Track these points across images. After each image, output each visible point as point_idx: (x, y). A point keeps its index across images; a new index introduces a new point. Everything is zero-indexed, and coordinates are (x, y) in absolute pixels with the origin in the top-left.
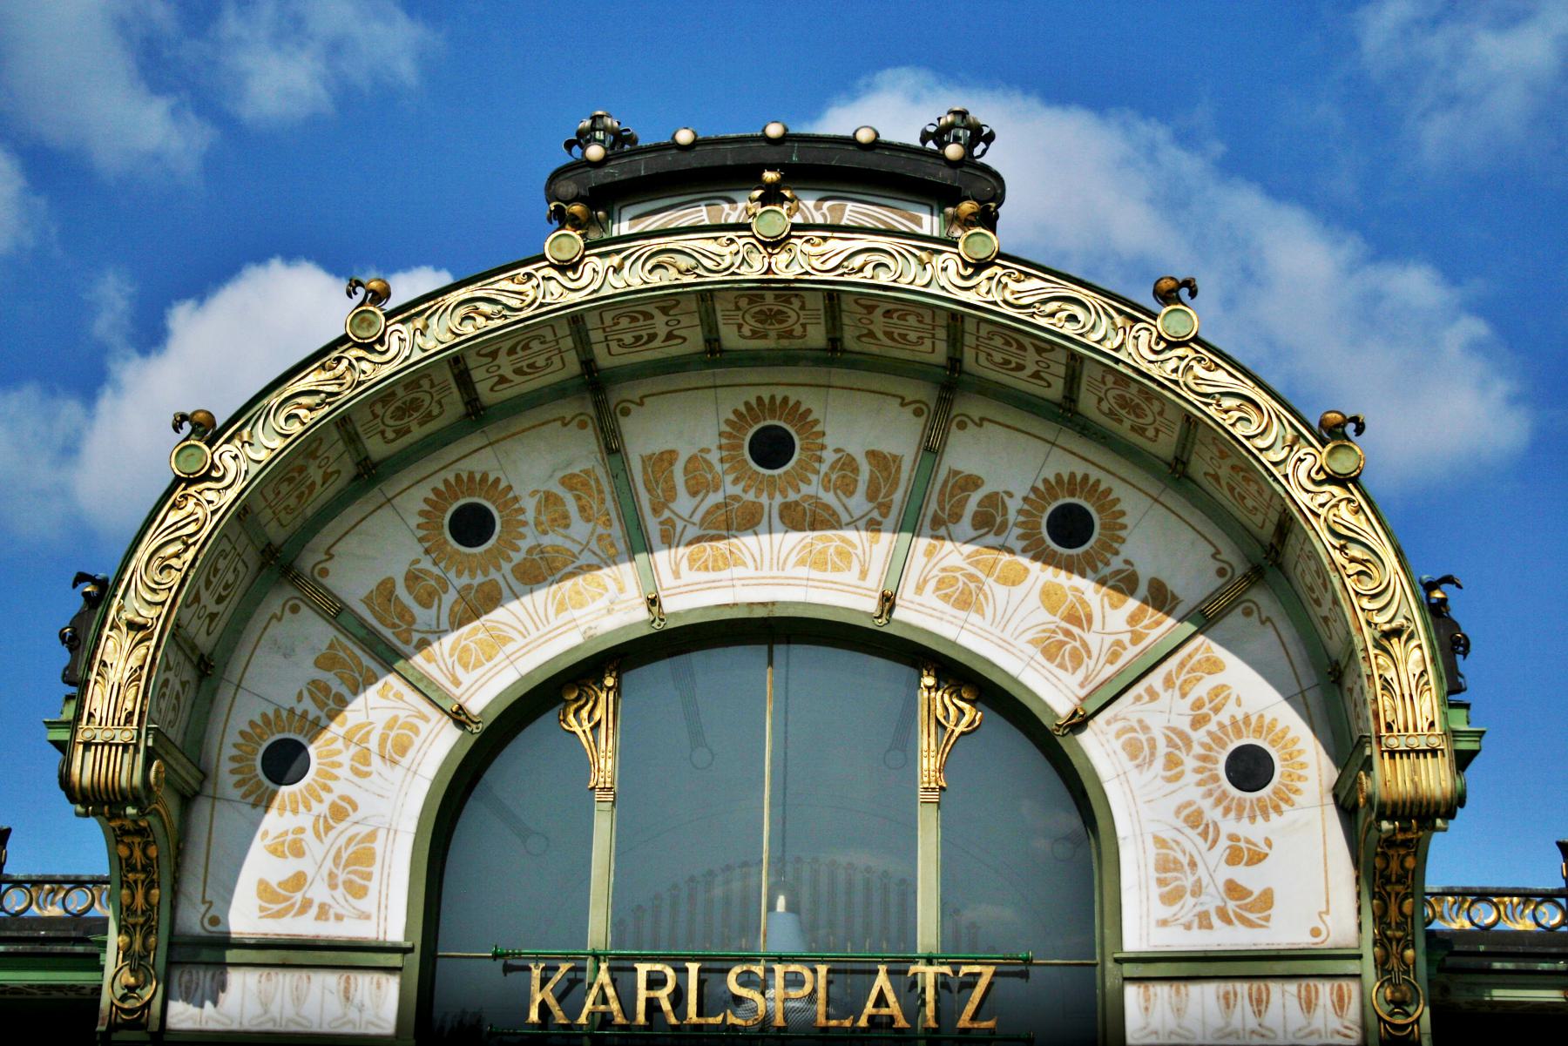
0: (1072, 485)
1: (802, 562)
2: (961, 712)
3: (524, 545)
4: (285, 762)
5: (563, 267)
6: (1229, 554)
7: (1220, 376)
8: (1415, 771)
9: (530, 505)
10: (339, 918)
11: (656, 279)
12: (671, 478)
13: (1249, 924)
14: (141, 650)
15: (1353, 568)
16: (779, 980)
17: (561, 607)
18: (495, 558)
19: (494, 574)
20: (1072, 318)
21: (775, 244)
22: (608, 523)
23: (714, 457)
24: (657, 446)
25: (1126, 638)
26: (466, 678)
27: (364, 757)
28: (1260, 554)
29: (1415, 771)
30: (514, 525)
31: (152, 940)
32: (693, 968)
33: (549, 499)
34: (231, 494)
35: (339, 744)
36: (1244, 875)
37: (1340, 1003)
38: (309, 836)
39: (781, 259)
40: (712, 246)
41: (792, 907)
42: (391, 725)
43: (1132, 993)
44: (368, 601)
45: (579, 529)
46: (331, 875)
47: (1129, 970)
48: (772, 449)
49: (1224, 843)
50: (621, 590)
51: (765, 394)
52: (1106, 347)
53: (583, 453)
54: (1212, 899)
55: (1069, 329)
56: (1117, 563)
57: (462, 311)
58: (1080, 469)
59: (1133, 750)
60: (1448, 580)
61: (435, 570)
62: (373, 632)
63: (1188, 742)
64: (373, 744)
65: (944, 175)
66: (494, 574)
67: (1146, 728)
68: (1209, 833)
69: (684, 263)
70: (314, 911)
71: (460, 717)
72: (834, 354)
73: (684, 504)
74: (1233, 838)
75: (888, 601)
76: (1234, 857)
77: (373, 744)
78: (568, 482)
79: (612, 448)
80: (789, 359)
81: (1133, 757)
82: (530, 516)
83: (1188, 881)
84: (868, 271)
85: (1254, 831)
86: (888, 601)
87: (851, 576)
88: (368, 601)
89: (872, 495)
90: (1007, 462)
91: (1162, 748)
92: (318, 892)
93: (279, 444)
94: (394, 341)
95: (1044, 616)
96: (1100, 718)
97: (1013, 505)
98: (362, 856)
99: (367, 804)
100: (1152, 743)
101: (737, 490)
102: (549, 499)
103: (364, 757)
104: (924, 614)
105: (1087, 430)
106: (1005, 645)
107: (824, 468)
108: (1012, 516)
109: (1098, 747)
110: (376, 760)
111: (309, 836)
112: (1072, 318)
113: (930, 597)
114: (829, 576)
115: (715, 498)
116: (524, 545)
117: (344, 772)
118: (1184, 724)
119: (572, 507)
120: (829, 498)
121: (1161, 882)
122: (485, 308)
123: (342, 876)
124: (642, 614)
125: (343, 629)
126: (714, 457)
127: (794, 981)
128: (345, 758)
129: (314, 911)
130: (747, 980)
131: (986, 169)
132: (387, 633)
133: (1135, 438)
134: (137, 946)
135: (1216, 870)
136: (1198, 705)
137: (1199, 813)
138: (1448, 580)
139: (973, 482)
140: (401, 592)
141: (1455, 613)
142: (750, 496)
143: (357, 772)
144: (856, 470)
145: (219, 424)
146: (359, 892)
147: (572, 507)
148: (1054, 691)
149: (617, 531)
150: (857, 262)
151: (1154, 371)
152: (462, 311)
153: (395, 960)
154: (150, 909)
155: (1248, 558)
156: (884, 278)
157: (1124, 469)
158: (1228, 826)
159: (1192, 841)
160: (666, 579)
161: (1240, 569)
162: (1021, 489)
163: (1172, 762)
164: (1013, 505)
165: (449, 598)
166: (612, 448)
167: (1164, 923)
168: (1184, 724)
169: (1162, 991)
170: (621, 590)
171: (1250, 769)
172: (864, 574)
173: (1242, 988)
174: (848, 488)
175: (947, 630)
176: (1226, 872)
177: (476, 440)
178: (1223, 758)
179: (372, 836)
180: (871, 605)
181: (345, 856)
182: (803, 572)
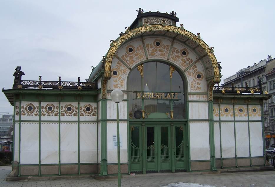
0: (184, 49)
1: (160, 55)
2: (173, 70)
3: (135, 52)
4: (115, 73)
5: (145, 27)
6: (198, 57)
7: (202, 42)
8: (217, 79)
9: (136, 48)
10: (121, 88)
11: (154, 29)
12: (149, 46)
13: (199, 90)
14: (109, 64)
15: (213, 61)
16: (160, 95)
17: (139, 59)
18: (133, 53)
19: (133, 55)
20: (190, 36)
21: (164, 26)
22: (143, 51)
23: (153, 44)
24: (148, 43)
25: (189, 64)
26: (131, 65)
27: (122, 73)
28: (200, 57)
29: (217, 79)
30: (134, 50)
31: (105, 90)
32: (152, 93)
33: (138, 48)
34: (116, 49)
35: (119, 71)
36: (198, 86)
37: (206, 97)
38: (118, 80)
39: (165, 28)
40: (159, 26)
41: (147, 85)
42: (124, 70)
43: (189, 96)
44: (121, 57)
45: (140, 51)
46: (120, 85)
47: (189, 94)
48: (158, 44)
49: (197, 83)
50: (144, 57)
51: (157, 39)
52: (193, 39)
53: (140, 43)
54: (195, 88)
55: (190, 37)
56: (188, 57)
57: (136, 31)
58: (185, 48)
59: (189, 74)
60: (220, 62)
61: (127, 54)
62: (122, 61)
63: (194, 74)
64: (123, 71)
65: (173, 18)
66: (133, 55)
67: (190, 72)
68: (195, 82)
69: (156, 28)
70: (119, 87)
71: (130, 69)
72: (164, 35)
73: (150, 49)
74: (197, 82)
75: (168, 59)
76: (197, 84)
77: (123, 71)
78: (139, 46)
79: (143, 43)
80: (159, 35)
81: (189, 75)
82: (136, 49)
83: (194, 86)
84: (173, 30)
85: (199, 82)
86: (168, 59)
87: (165, 57)
88: (121, 57)
89: (167, 49)
90: (179, 47)
91: (191, 74)
92: (119, 86)
93: (120, 43)
94: (130, 34)
95: (182, 62)
96: (186, 71)
97: (179, 51)
98: (123, 82)
99: (122, 77)
100: (191, 74)
101: (155, 48)
102: (138, 48)
103: (122, 73)
104: (171, 61)
105: (186, 44)
106: (178, 64)
107: (163, 46)
108: (179, 52)
109: (186, 74)
110: (123, 73)
111: (118, 80)
112: (190, 36)
113: (172, 59)
114: (163, 57)
115: (153, 49)
116: (135, 52)
117: (120, 74)
118: (193, 72)
119: (140, 48)
120: (163, 49)
121: (191, 86)
122: (138, 31)
123: (121, 84)
124: (146, 60)
125: (120, 60)
126: (153, 44)
127: (161, 94)
128: (120, 73)
129: (119, 87)
130: (157, 94)
131: (178, 18)
132: (123, 60)
133: (191, 46)
134: (104, 91)
135: (196, 85)
136: (195, 70)
137: (195, 80)
138: (220, 62)
139: (176, 49)
140: (124, 56)
141: (220, 65)
142: (156, 49)
143: (121, 74)
144: (165, 47)
145: (115, 41)
146: (123, 86)
147: (140, 48)
148: (182, 68)
149: (144, 51)
150: (172, 29)
151: (197, 41)
152: (136, 31)
153: (126, 92)
154: (105, 87)
155: (199, 57)
156: (174, 31)
157: (189, 48)
158: (197, 82)
159: (194, 83)
160: (149, 56)
161: (198, 58)
162: (180, 50)
163: (192, 76)
164: (179, 51)
165: (129, 57)
166: (143, 43)
167: (192, 90)
168: (193, 72)
169: (192, 96)
170: (144, 57)
171: (199, 76)
172: (166, 57)
173: (198, 96)
174: (165, 48)
175: (173, 62)
176: (197, 86)
177: (131, 42)
178: (197, 75)
179: (123, 80)
180: (167, 60)
181: (121, 82)
182: (161, 56)
